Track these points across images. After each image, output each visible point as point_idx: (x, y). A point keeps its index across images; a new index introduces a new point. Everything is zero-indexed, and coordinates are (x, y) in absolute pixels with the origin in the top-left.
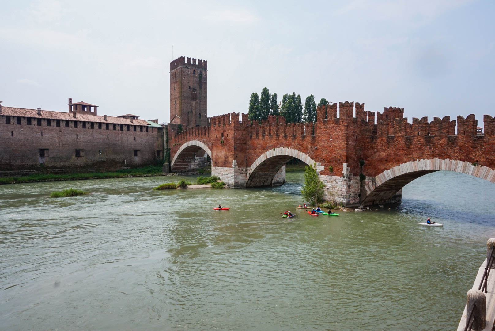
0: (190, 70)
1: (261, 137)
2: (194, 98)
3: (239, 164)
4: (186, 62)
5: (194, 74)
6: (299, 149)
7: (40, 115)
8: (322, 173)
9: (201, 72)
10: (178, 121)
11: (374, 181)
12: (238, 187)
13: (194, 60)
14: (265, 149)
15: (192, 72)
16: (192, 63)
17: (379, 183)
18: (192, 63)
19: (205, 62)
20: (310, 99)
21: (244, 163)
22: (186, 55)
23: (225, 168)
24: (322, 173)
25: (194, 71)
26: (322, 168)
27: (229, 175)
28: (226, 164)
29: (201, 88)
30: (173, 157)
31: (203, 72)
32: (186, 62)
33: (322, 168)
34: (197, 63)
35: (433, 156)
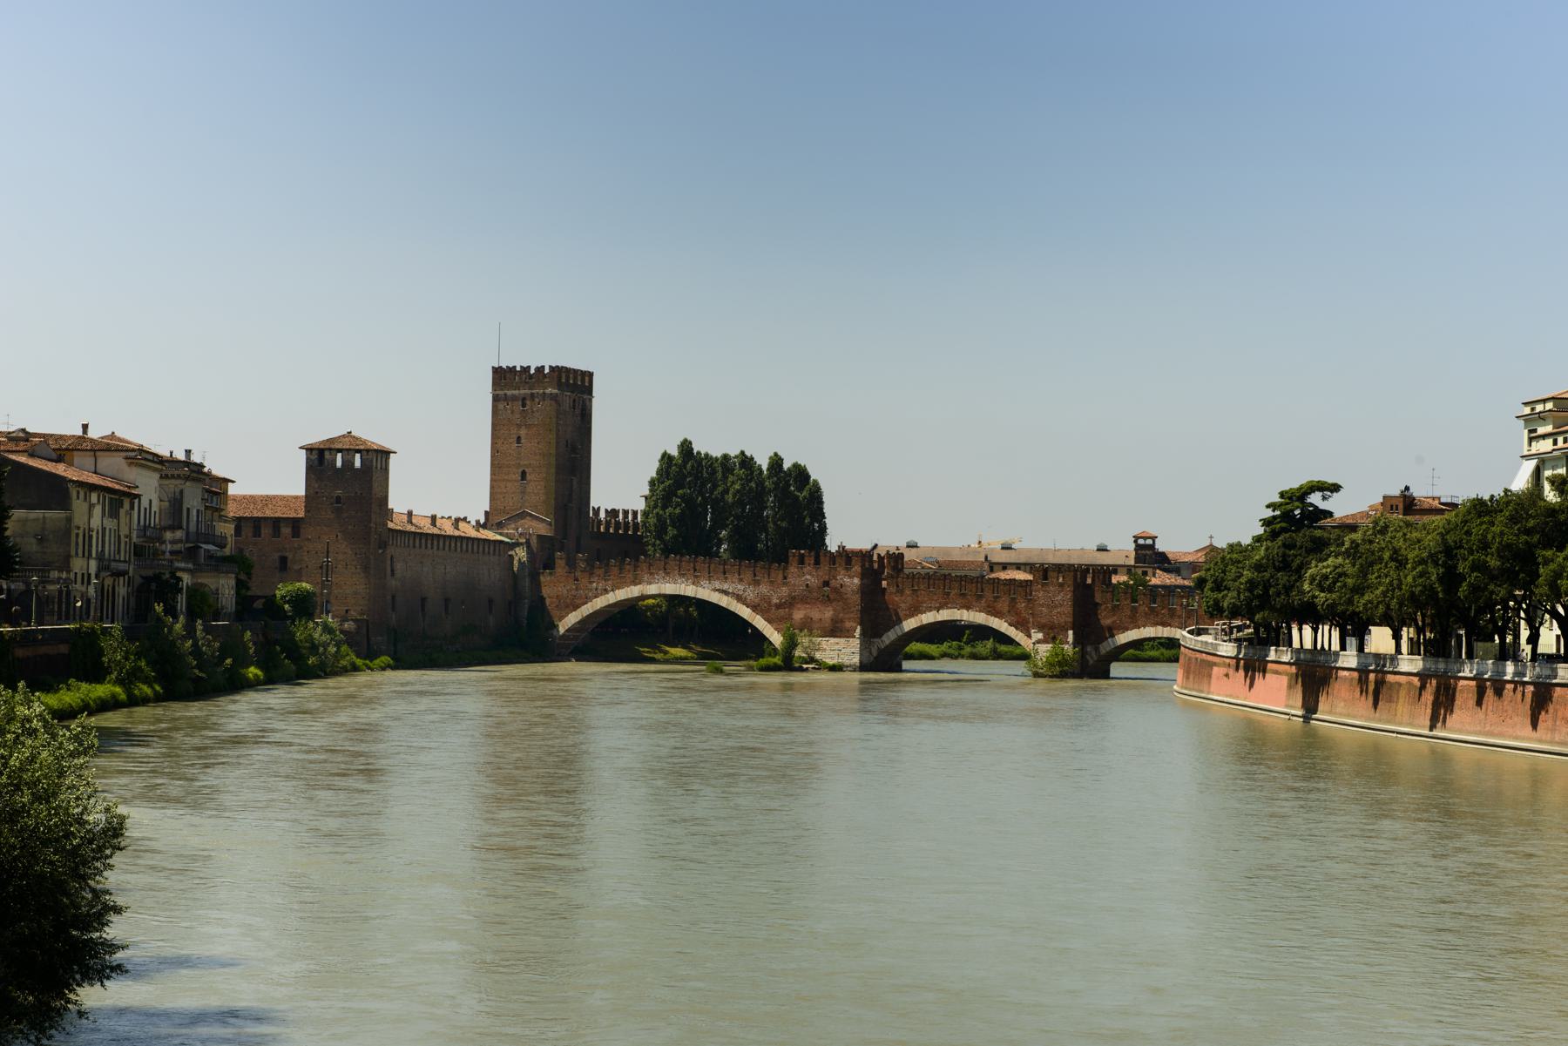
1: (908, 592)
3: (863, 634)
6: (988, 613)
7: (410, 522)
8: (1039, 642)
10: (544, 530)
11: (1097, 650)
12: (863, 667)
14: (915, 610)
17: (1103, 652)
19: (591, 375)
20: (776, 462)
21: (872, 630)
23: (833, 640)
24: (1039, 642)
26: (1040, 636)
27: (849, 650)
28: (835, 630)
30: (561, 618)
33: (1040, 636)
35: (1155, 624)
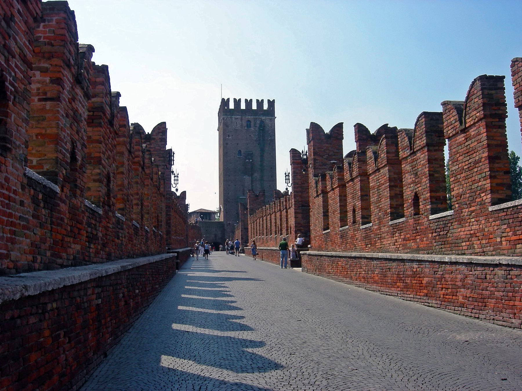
0: (239, 122)
2: (249, 170)
4: (232, 106)
5: (249, 126)
9: (262, 122)
13: (249, 103)
15: (245, 124)
16: (243, 106)
18: (243, 106)
19: (271, 104)
22: (231, 95)
25: (249, 121)
29: (262, 150)
31: (267, 122)
32: (232, 106)
34: (254, 107)
